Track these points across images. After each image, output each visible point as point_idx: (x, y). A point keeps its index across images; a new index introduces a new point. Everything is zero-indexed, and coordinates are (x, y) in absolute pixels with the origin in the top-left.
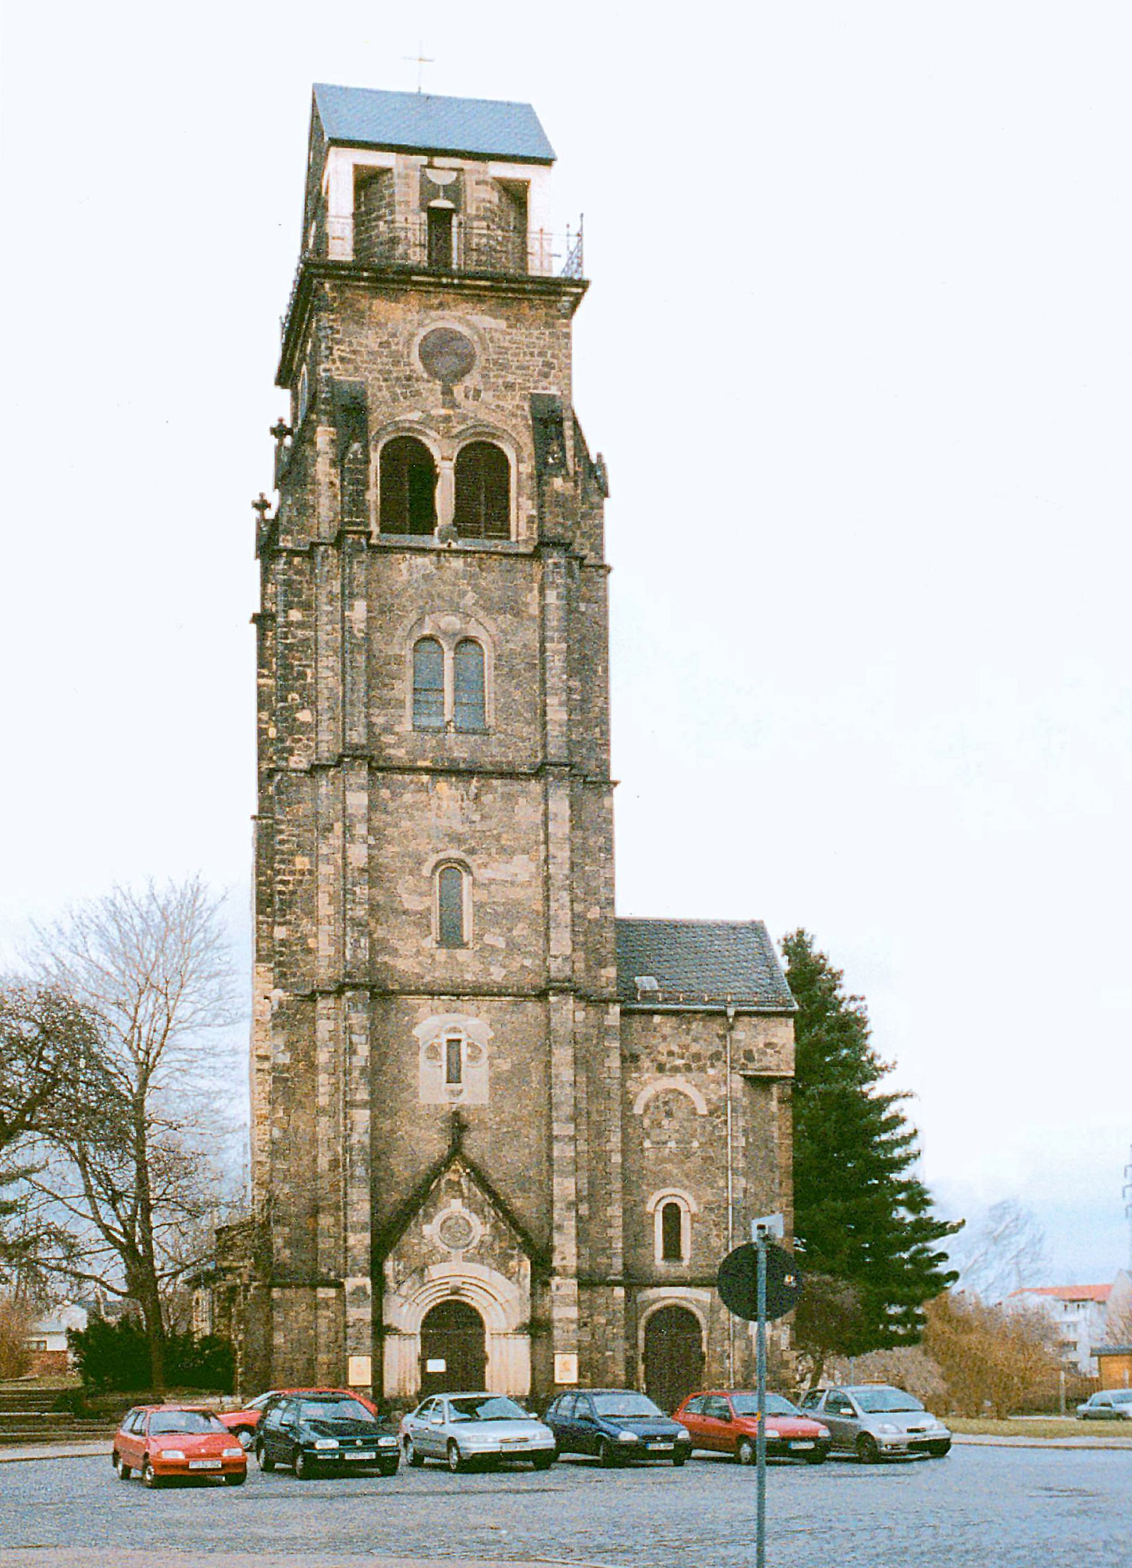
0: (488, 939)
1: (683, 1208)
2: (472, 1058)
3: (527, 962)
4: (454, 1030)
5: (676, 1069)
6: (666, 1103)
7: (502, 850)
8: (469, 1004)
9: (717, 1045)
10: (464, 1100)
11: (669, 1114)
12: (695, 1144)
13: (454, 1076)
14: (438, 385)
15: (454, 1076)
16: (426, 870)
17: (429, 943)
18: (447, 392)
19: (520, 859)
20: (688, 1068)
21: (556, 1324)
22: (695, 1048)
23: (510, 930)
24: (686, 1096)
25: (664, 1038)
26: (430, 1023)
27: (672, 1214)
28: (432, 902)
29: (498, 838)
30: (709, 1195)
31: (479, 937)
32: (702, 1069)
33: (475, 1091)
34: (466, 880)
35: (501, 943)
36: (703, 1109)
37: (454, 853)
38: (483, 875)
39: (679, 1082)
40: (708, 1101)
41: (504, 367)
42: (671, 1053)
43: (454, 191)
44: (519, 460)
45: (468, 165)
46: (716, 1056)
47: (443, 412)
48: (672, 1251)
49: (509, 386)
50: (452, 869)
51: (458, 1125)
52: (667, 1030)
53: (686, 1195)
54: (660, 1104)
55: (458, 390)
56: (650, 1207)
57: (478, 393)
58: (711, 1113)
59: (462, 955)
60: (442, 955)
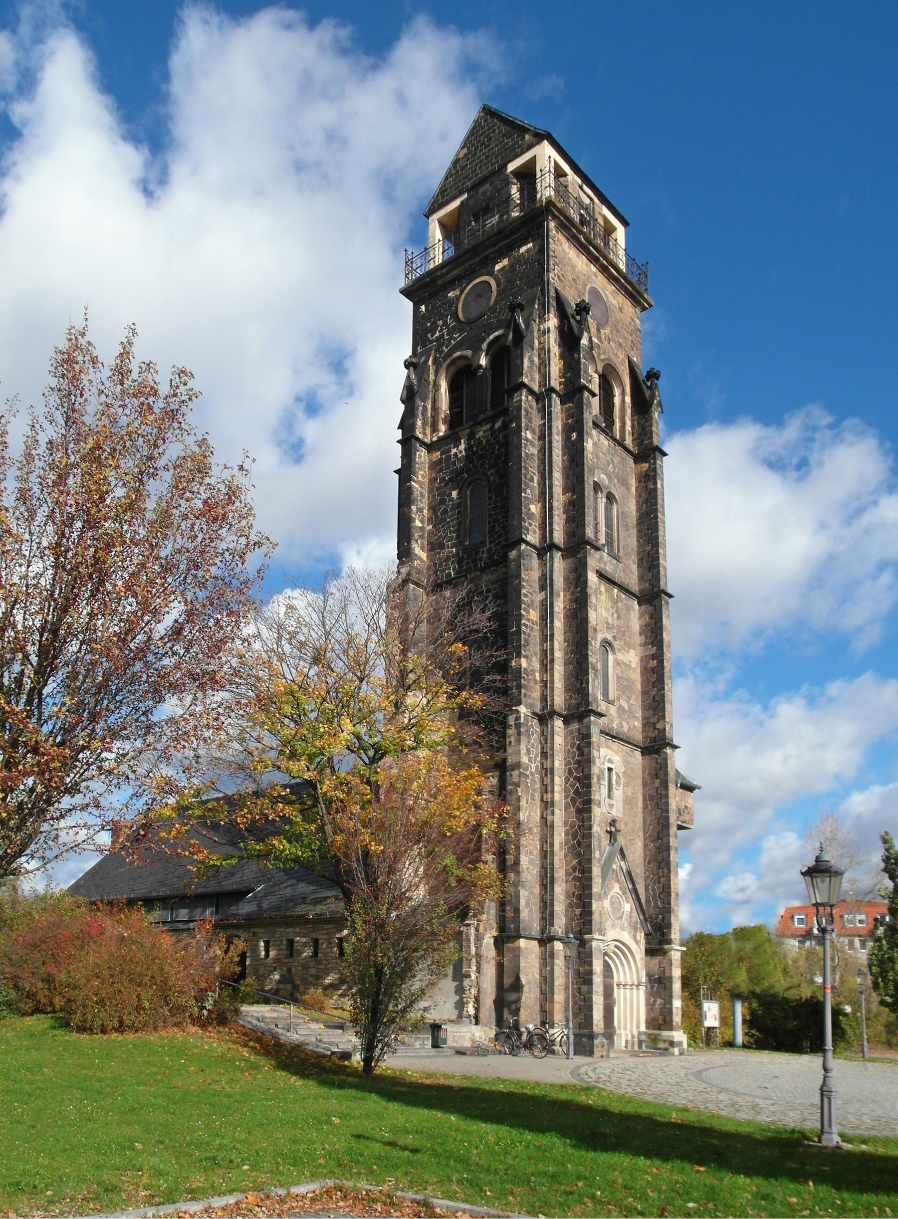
3: (636, 724)
4: (610, 761)
8: (616, 745)
10: (614, 812)
19: (632, 652)
23: (630, 699)
29: (624, 633)
34: (611, 657)
37: (609, 637)
38: (620, 656)
41: (618, 331)
49: (620, 345)
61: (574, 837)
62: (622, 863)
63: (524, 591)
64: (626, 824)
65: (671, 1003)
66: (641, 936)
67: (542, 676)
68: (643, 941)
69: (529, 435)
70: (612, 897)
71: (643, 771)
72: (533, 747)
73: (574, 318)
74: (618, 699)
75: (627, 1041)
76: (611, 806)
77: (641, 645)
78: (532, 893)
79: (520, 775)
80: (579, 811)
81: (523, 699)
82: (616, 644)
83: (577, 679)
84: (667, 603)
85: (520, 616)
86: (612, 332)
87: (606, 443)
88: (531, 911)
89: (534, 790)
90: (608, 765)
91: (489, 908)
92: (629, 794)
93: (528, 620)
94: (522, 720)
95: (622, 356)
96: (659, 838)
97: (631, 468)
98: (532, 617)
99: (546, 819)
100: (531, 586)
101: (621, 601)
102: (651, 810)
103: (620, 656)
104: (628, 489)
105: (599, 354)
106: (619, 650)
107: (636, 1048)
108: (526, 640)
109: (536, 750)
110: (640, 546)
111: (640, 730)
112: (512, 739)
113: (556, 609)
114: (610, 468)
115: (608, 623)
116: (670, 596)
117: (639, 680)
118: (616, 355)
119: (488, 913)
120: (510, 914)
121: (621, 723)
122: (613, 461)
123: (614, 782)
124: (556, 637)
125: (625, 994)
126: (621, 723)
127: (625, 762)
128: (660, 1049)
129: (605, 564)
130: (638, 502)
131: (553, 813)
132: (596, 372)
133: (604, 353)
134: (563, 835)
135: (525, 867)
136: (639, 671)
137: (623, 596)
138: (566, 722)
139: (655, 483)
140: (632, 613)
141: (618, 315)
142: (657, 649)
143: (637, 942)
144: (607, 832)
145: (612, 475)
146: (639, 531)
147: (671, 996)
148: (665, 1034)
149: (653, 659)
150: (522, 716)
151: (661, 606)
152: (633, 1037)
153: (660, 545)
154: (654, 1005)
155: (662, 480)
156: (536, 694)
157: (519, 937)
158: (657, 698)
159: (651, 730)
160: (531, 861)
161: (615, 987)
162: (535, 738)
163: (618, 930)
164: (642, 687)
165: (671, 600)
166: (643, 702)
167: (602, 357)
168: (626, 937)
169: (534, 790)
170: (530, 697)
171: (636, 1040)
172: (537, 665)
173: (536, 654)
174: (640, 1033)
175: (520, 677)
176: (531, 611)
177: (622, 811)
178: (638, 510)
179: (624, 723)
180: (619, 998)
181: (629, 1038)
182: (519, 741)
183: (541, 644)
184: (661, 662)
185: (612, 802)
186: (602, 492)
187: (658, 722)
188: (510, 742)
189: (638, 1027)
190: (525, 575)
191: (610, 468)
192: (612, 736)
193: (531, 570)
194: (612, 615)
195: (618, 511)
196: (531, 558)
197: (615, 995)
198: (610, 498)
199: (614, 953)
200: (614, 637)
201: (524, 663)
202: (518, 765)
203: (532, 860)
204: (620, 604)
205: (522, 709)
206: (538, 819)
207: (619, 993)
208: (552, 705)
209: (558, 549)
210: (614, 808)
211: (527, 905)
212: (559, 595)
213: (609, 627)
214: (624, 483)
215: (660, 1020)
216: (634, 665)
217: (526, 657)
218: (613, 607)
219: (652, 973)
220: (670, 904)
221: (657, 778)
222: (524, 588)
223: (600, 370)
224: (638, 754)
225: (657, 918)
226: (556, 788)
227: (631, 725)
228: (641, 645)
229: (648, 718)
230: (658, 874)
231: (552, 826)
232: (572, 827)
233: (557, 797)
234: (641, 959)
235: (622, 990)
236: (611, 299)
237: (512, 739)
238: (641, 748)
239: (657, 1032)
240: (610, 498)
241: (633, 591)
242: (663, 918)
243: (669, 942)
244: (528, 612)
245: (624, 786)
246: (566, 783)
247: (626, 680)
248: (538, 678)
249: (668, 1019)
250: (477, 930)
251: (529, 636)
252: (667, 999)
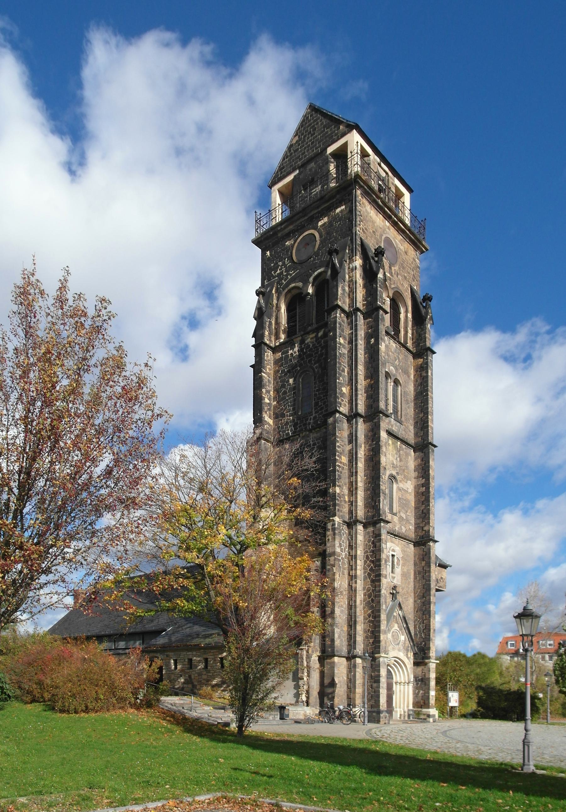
3: (411, 527)
4: (393, 550)
8: (397, 540)
10: (395, 581)
19: (409, 482)
23: (407, 512)
33: (397, 581)
34: (395, 486)
37: (394, 473)
38: (401, 485)
41: (404, 268)
49: (405, 278)
57: (398, 274)
61: (370, 596)
62: (400, 612)
63: (338, 444)
65: (429, 693)
66: (411, 655)
67: (349, 498)
68: (412, 658)
69: (342, 341)
70: (393, 632)
71: (415, 557)
73: (373, 259)
74: (399, 512)
75: (401, 715)
76: (394, 578)
77: (415, 478)
78: (342, 630)
79: (335, 559)
80: (373, 581)
81: (337, 513)
82: (398, 478)
83: (373, 500)
84: (433, 451)
85: (335, 460)
86: (399, 268)
87: (394, 345)
88: (341, 640)
89: (344, 569)
90: (391, 553)
91: (315, 639)
92: (405, 570)
93: (341, 462)
94: (336, 526)
95: (406, 285)
96: (423, 597)
97: (411, 362)
98: (343, 461)
99: (352, 586)
100: (342, 441)
101: (403, 450)
102: (419, 580)
103: (401, 485)
104: (409, 376)
105: (390, 284)
106: (401, 481)
107: (406, 718)
108: (339, 476)
109: (345, 544)
110: (416, 414)
111: (413, 531)
112: (330, 538)
113: (359, 455)
114: (397, 362)
115: (393, 464)
116: (435, 446)
117: (414, 500)
118: (402, 285)
119: (315, 642)
120: (328, 642)
121: (401, 527)
122: (398, 358)
123: (396, 563)
124: (359, 473)
125: (400, 687)
126: (401, 527)
127: (403, 551)
128: (421, 719)
129: (392, 426)
130: (415, 385)
131: (356, 582)
132: (388, 297)
133: (394, 283)
134: (362, 595)
135: (338, 615)
136: (413, 494)
137: (404, 447)
138: (365, 526)
139: (427, 372)
140: (410, 457)
141: (404, 257)
142: (426, 480)
143: (408, 658)
144: (391, 593)
145: (398, 367)
146: (415, 404)
147: (429, 689)
148: (424, 710)
149: (423, 487)
150: (336, 523)
151: (429, 453)
152: (404, 712)
153: (429, 413)
154: (418, 694)
155: (432, 370)
156: (346, 509)
157: (334, 656)
158: (425, 511)
159: (421, 531)
160: (342, 612)
161: (394, 684)
162: (345, 537)
163: (397, 651)
164: (415, 504)
165: (435, 449)
166: (415, 513)
167: (393, 286)
168: (402, 655)
169: (344, 569)
170: (341, 511)
171: (406, 714)
172: (346, 491)
173: (345, 484)
174: (409, 710)
175: (335, 499)
176: (343, 457)
177: (400, 581)
178: (415, 390)
179: (402, 527)
180: (396, 691)
181: (402, 713)
182: (334, 539)
183: (349, 478)
184: (428, 488)
185: (394, 575)
186: (391, 378)
187: (425, 526)
188: (329, 539)
189: (408, 707)
190: (339, 434)
191: (397, 362)
192: (395, 535)
193: (343, 430)
194: (396, 459)
195: (401, 391)
196: (343, 422)
197: (394, 689)
198: (396, 382)
199: (394, 664)
200: (397, 473)
201: (338, 490)
202: (334, 553)
203: (343, 610)
204: (401, 452)
205: (337, 519)
206: (346, 586)
207: (396, 688)
208: (356, 516)
209: (361, 416)
210: (395, 579)
212: (361, 447)
213: (394, 467)
214: (406, 372)
215: (421, 702)
216: (410, 491)
217: (339, 486)
218: (397, 454)
219: (417, 676)
220: (430, 636)
221: (423, 560)
222: (338, 442)
223: (391, 295)
224: (411, 546)
225: (421, 644)
226: (358, 567)
227: (408, 528)
228: (415, 478)
229: (419, 524)
230: (423, 618)
231: (355, 590)
232: (368, 590)
233: (359, 572)
234: (411, 668)
235: (398, 686)
236: (400, 246)
237: (330, 538)
238: (413, 542)
239: (420, 709)
240: (396, 382)
241: (410, 443)
242: (425, 644)
243: (429, 658)
244: (341, 458)
245: (402, 566)
246: (365, 564)
247: (405, 500)
248: (347, 499)
249: (426, 702)
250: (307, 652)
251: (341, 473)
252: (426, 690)
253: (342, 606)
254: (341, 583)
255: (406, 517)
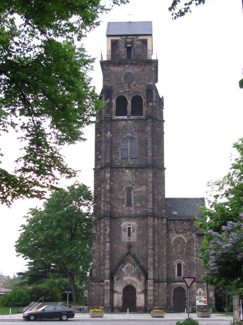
0: (137, 205)
1: (182, 264)
2: (133, 231)
4: (129, 225)
5: (180, 233)
6: (178, 240)
7: (140, 184)
9: (189, 227)
10: (131, 240)
11: (179, 243)
12: (185, 250)
13: (129, 235)
14: (127, 84)
15: (129, 235)
16: (124, 190)
17: (124, 206)
18: (129, 85)
20: (183, 232)
21: (149, 291)
22: (185, 228)
23: (141, 202)
24: (182, 238)
25: (178, 225)
26: (125, 224)
27: (179, 265)
28: (125, 197)
30: (187, 261)
31: (135, 204)
32: (186, 232)
34: (132, 191)
35: (139, 205)
36: (186, 242)
37: (130, 186)
38: (136, 190)
39: (181, 235)
40: (187, 240)
42: (179, 229)
43: (132, 43)
44: (144, 99)
45: (134, 37)
46: (189, 229)
47: (128, 90)
48: (179, 274)
49: (142, 83)
50: (129, 190)
51: (130, 246)
52: (178, 224)
53: (182, 261)
54: (177, 240)
55: (131, 85)
56: (174, 264)
57: (135, 85)
58: (188, 242)
59: (132, 208)
60: (127, 209)
64: (138, 243)
72: (98, 227)
82: (134, 187)
98: (99, 190)
103: (136, 190)
106: (136, 188)
121: (136, 211)
191: (133, 130)
194: (133, 178)
210: (132, 239)
211: (96, 272)
245: (137, 231)
253: (98, 258)
254: (97, 247)
255: (141, 205)
